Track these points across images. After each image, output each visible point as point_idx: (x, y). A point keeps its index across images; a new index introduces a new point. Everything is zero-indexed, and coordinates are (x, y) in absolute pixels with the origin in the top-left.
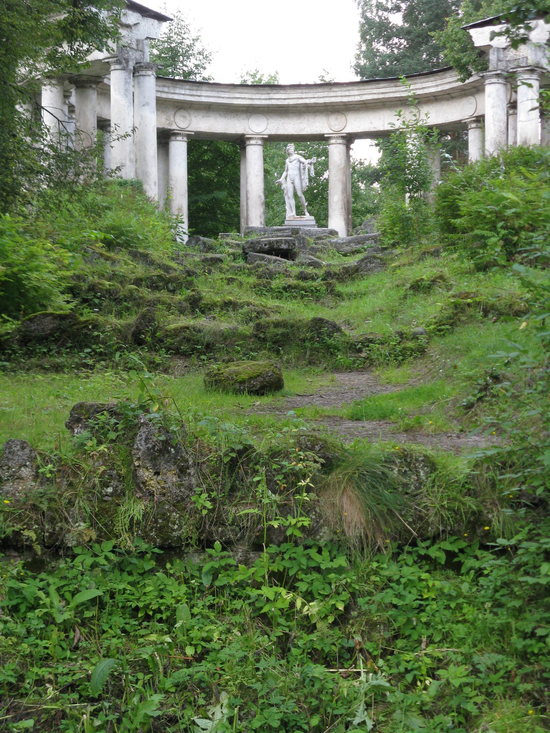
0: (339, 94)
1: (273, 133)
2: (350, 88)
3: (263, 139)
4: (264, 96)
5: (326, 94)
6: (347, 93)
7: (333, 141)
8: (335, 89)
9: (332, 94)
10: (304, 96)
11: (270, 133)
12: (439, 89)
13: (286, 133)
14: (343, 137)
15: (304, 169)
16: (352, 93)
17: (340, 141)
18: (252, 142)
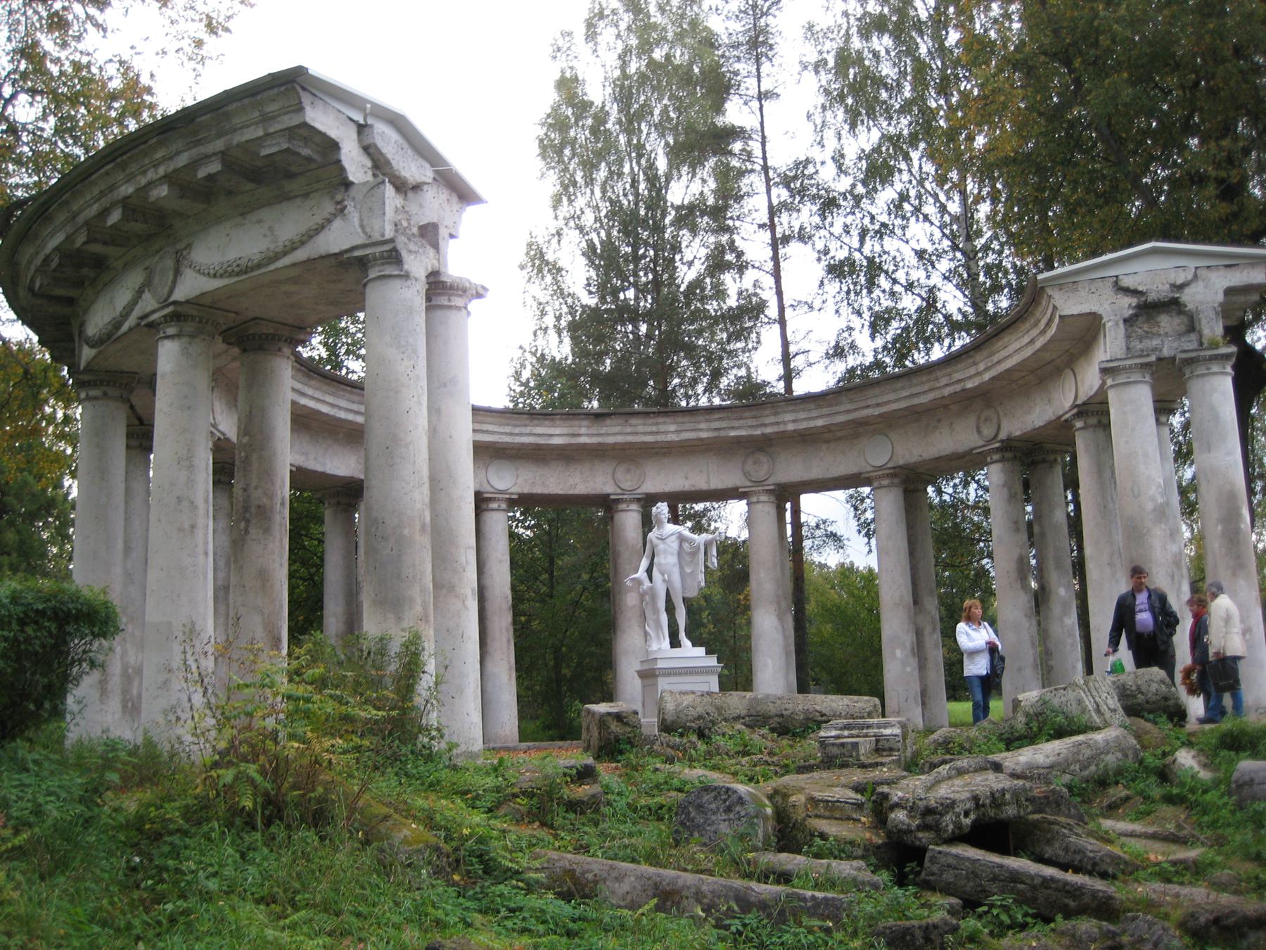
0: (641, 429)
1: (526, 491)
2: (661, 420)
3: (510, 499)
4: (517, 430)
5: (617, 429)
6: (654, 429)
7: (623, 506)
8: (633, 421)
9: (629, 430)
10: (583, 431)
11: (520, 491)
12: (820, 423)
13: (546, 491)
14: (639, 500)
15: (694, 554)
16: (663, 428)
17: (634, 506)
18: (494, 505)
